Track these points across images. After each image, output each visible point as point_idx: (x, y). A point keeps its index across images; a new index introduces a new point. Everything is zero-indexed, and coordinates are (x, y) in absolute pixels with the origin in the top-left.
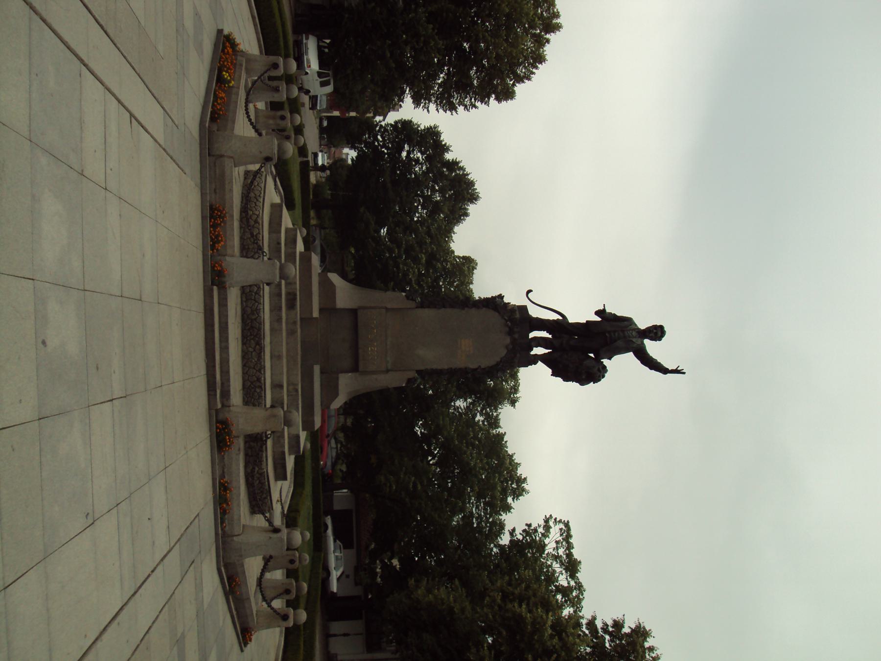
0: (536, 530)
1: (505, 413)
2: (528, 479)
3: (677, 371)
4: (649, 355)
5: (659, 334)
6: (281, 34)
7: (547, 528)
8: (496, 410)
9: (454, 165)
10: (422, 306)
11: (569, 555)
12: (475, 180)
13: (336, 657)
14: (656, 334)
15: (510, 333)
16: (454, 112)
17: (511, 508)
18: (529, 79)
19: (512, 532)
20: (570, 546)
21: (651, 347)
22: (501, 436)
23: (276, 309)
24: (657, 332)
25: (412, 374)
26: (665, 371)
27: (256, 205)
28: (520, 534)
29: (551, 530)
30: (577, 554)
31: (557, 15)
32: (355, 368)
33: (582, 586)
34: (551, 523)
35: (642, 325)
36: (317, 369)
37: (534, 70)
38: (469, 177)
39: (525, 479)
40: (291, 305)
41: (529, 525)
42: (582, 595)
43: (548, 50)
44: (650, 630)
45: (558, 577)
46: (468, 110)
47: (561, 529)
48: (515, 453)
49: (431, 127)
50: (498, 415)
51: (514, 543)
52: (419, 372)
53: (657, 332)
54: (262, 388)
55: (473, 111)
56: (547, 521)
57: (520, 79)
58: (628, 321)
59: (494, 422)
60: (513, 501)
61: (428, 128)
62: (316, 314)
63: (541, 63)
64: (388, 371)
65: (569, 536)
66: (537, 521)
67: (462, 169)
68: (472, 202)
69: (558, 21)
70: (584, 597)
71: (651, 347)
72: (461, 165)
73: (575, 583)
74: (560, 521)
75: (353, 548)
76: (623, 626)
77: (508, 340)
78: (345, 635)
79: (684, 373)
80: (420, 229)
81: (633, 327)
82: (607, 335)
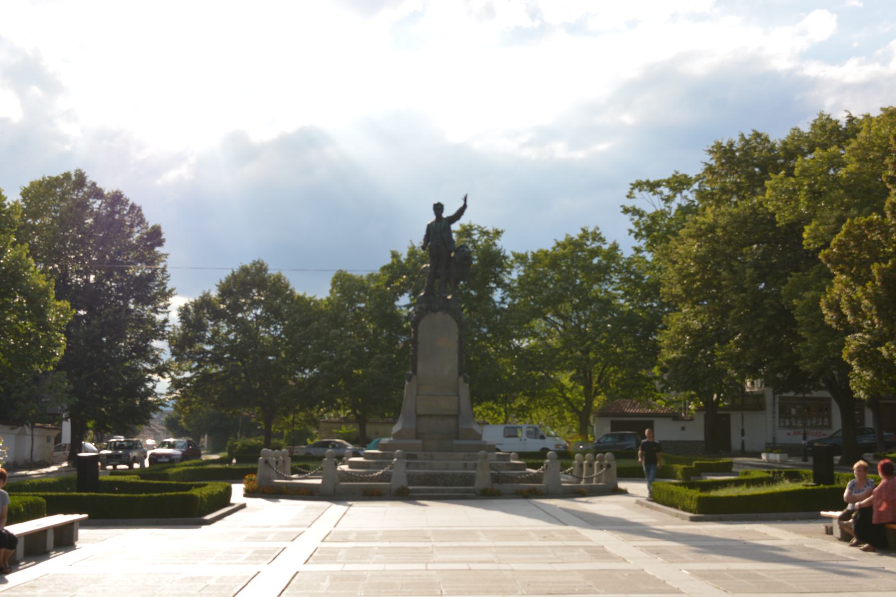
0: (637, 224)
1: (507, 246)
2: (583, 227)
3: (465, 199)
5: (440, 207)
6: (200, 467)
7: (635, 212)
8: (505, 257)
9: (226, 290)
10: (415, 371)
11: (668, 182)
12: (241, 265)
14: (439, 209)
15: (435, 311)
16: (174, 292)
17: (614, 243)
18: (140, 210)
19: (638, 250)
20: (658, 184)
21: (447, 213)
22: (535, 256)
23: (417, 466)
25: (461, 379)
26: (464, 207)
28: (639, 241)
29: (637, 207)
30: (667, 175)
31: (67, 176)
32: (456, 417)
33: (699, 175)
34: (629, 204)
35: (432, 218)
36: (455, 442)
37: (130, 203)
38: (235, 270)
39: (583, 230)
40: (414, 457)
41: (631, 231)
43: (108, 186)
44: (715, 142)
45: (690, 201)
46: (168, 276)
47: (640, 191)
48: (555, 240)
49: (179, 315)
50: (514, 254)
51: (650, 247)
52: (460, 374)
54: (466, 475)
55: (169, 271)
56: (626, 211)
57: (142, 221)
58: (429, 227)
59: (521, 258)
60: (605, 244)
61: (182, 318)
62: (420, 442)
63: (121, 196)
64: (458, 395)
65: (648, 183)
66: (627, 222)
67: (228, 280)
68: (266, 270)
69: (73, 173)
71: (447, 213)
72: (224, 280)
73: (695, 182)
74: (631, 193)
76: (710, 166)
77: (440, 313)
79: (467, 195)
80: (300, 334)
81: (434, 225)
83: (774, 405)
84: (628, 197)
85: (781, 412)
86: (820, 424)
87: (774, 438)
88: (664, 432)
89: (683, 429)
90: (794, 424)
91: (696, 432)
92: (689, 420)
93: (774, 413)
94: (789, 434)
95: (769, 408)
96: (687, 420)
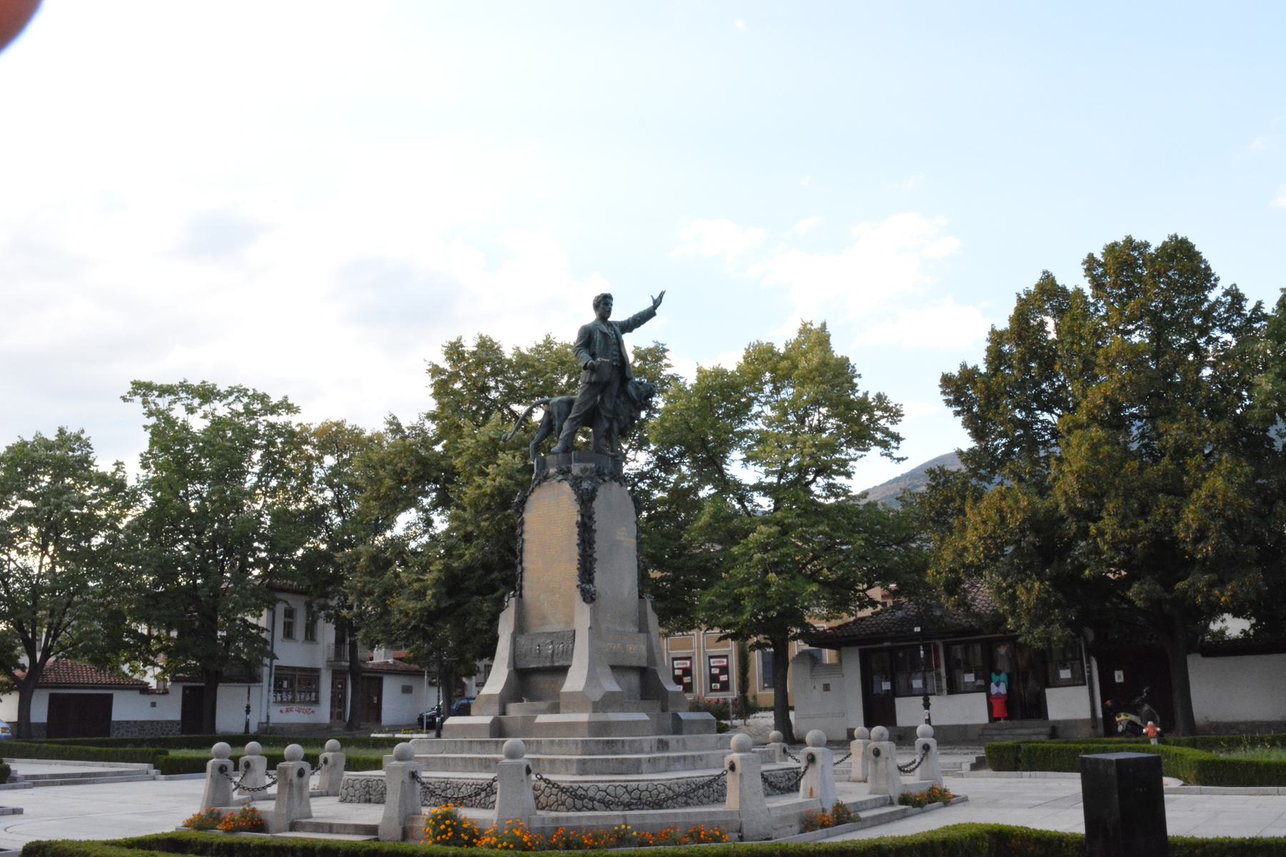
4: (628, 321)
13: (262, 723)
21: (618, 314)
24: (603, 304)
27: (647, 790)
35: (590, 317)
42: (248, 390)
53: (603, 304)
70: (254, 389)
71: (618, 314)
75: (111, 696)
78: (248, 710)
82: (615, 364)
83: (270, 676)
84: (124, 399)
85: (275, 686)
86: (308, 699)
87: (268, 717)
88: (126, 709)
89: (153, 705)
90: (285, 700)
91: (170, 710)
92: (164, 694)
93: (270, 685)
94: (281, 711)
95: (265, 679)
96: (159, 694)
